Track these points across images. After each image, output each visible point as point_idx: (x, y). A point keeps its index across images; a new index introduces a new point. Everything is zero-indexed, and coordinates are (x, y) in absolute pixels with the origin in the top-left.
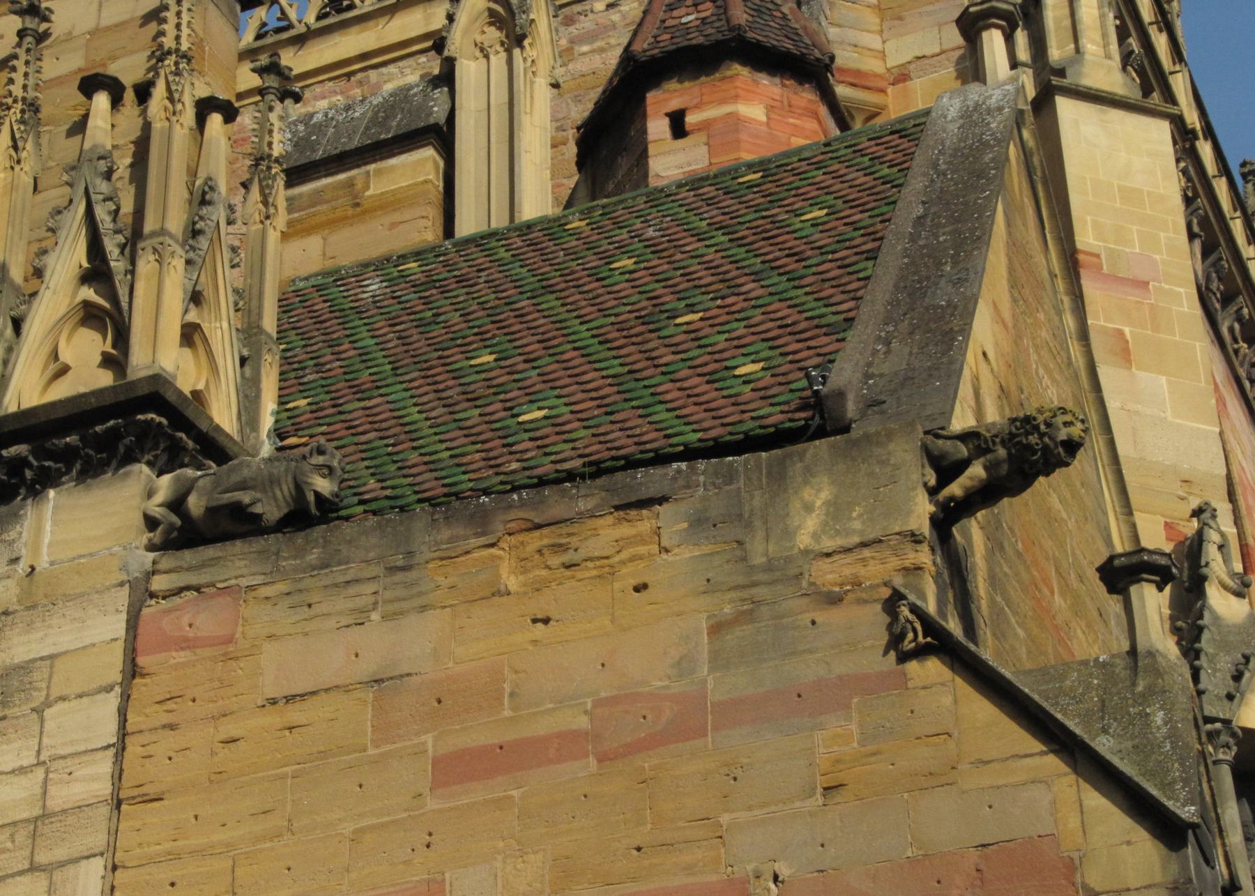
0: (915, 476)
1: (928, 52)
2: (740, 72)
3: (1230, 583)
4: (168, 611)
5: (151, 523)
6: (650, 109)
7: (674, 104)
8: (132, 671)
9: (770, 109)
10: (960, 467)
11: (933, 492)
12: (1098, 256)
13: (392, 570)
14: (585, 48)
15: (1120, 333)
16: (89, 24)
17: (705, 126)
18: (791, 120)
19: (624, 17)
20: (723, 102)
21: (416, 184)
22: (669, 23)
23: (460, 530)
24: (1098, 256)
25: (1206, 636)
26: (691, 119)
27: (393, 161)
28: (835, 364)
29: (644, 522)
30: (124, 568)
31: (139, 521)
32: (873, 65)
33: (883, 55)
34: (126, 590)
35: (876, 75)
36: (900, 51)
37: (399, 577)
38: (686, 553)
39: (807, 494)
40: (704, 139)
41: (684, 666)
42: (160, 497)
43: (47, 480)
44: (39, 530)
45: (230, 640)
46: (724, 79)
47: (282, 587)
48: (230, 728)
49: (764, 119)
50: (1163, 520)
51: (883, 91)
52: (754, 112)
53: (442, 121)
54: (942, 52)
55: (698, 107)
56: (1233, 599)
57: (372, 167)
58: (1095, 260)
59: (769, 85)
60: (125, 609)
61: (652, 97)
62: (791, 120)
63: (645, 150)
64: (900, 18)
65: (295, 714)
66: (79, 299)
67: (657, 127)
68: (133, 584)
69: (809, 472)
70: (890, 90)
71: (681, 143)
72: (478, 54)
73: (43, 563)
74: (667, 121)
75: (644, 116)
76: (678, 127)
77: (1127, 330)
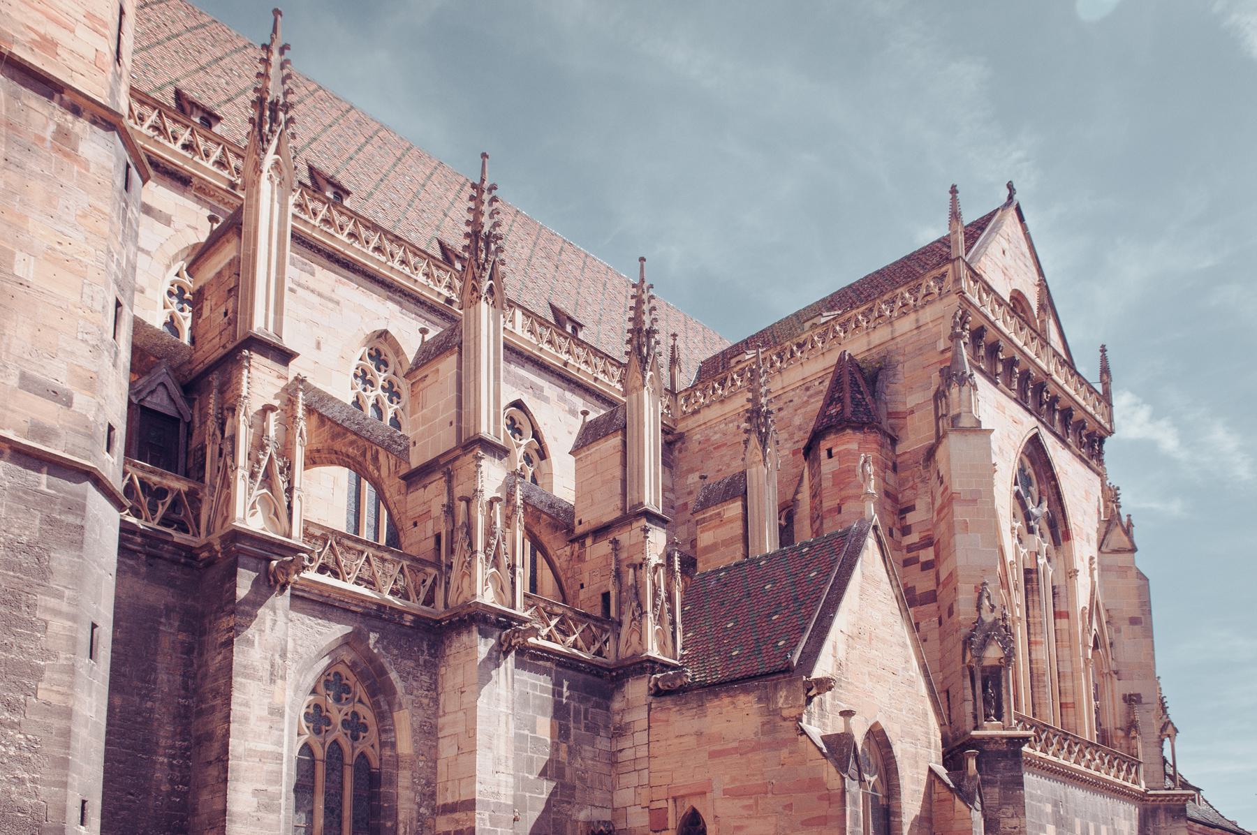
5: (650, 689)
7: (829, 446)
8: (649, 727)
9: (859, 444)
13: (699, 706)
14: (813, 400)
15: (965, 520)
17: (839, 453)
23: (712, 697)
26: (834, 451)
38: (756, 706)
41: (756, 734)
45: (668, 721)
47: (678, 708)
48: (669, 742)
65: (682, 740)
67: (824, 454)
76: (830, 455)
77: (968, 519)
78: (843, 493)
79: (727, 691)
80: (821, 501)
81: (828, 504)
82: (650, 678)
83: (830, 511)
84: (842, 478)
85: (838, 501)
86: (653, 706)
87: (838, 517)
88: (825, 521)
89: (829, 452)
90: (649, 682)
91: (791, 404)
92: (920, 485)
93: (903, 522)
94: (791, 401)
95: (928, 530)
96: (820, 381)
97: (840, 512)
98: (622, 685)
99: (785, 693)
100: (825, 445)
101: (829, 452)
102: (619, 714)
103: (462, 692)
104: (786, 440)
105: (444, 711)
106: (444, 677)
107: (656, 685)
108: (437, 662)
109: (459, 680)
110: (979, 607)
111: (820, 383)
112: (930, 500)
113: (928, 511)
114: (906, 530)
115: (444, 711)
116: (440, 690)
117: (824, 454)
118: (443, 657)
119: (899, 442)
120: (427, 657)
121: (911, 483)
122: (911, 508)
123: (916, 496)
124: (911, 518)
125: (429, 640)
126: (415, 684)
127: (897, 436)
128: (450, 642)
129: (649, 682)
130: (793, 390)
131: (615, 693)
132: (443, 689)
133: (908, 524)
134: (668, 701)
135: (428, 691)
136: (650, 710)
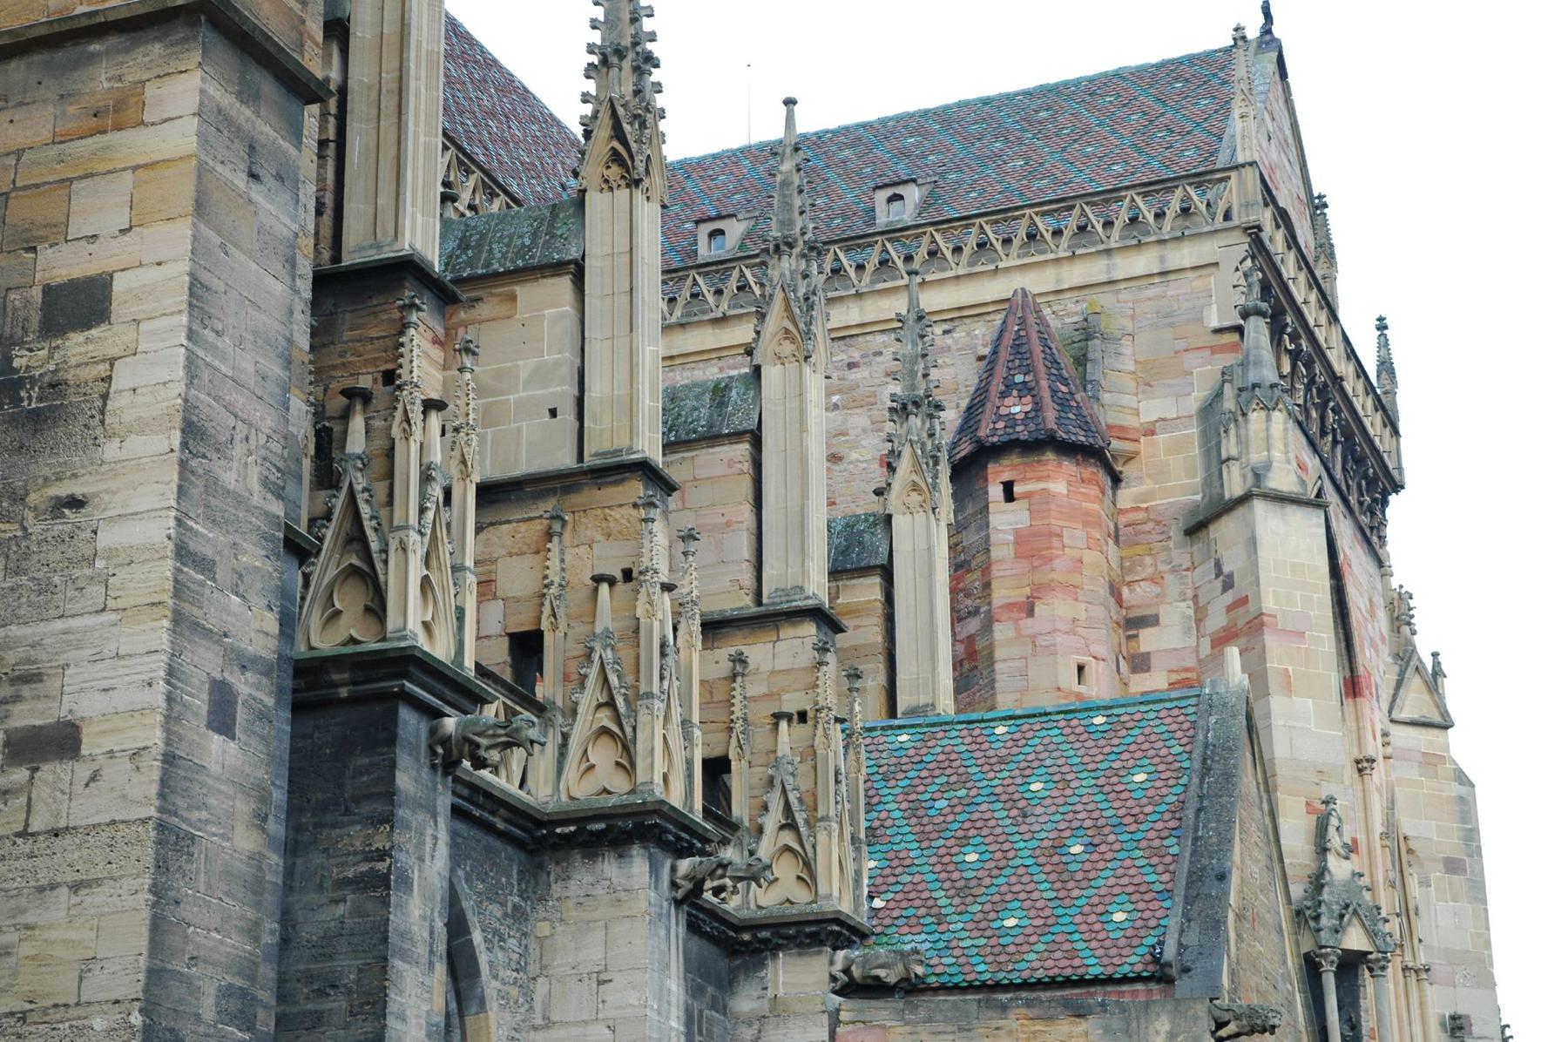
0: (1206, 1025)
1: (1169, 417)
2: (1050, 456)
3: (1342, 852)
4: (851, 1032)
5: (834, 978)
6: (990, 477)
7: (1006, 477)
10: (1226, 1024)
11: (1213, 1033)
12: (1275, 617)
13: (961, 1029)
15: (1286, 670)
16: (769, 667)
17: (1028, 495)
18: (1083, 490)
19: (956, 342)
20: (1040, 479)
21: (870, 601)
22: (1003, 411)
24: (1275, 617)
25: (1326, 890)
26: (1017, 489)
27: (854, 582)
28: (1027, 289)
29: (1082, 1026)
30: (824, 1003)
31: (826, 977)
32: (1129, 421)
33: (1137, 413)
34: (826, 1016)
35: (1134, 429)
36: (1151, 410)
37: (965, 1034)
39: (1158, 1025)
40: (1027, 506)
42: (839, 966)
43: (778, 947)
44: (776, 975)
46: (1039, 462)
47: (908, 1029)
49: (1065, 492)
50: (1304, 800)
51: (1137, 441)
52: (1059, 487)
53: (885, 562)
54: (1178, 418)
55: (1024, 480)
56: (1344, 861)
57: (841, 583)
58: (1272, 619)
59: (1069, 466)
60: (827, 1025)
61: (991, 467)
62: (1083, 490)
63: (987, 507)
64: (1150, 386)
66: (780, 844)
67: (995, 491)
68: (830, 1015)
69: (1158, 1014)
70: (1142, 439)
71: (1010, 506)
72: (906, 511)
73: (781, 993)
74: (1001, 487)
75: (986, 480)
76: (1009, 496)
77: (1290, 668)
78: (1039, 577)
79: (1029, 1004)
80: (987, 585)
81: (1002, 594)
82: (832, 957)
83: (1010, 607)
84: (1032, 547)
85: (1027, 591)
86: (844, 1016)
87: (1028, 625)
88: (997, 627)
89: (1008, 487)
90: (832, 963)
91: (879, 359)
92: (1169, 578)
93: (1133, 644)
94: (880, 353)
95: (1187, 670)
96: (946, 326)
97: (1031, 613)
98: (761, 965)
99: (1167, 1027)
100: (998, 472)
101: (1008, 487)
102: (750, 1024)
103: (600, 983)
104: (865, 431)
105: (546, 1018)
106: (547, 942)
107: (847, 971)
108: (528, 909)
109: (592, 954)
110: (1322, 850)
111: (946, 332)
112: (1191, 612)
113: (1187, 631)
114: (1140, 663)
115: (546, 1018)
116: (533, 969)
117: (995, 491)
118: (542, 899)
119: (1123, 484)
120: (517, 899)
121: (1150, 570)
122: (1149, 621)
123: (1161, 597)
124: (1148, 640)
125: (520, 863)
126: (500, 955)
127: (1121, 472)
128: (565, 870)
129: (832, 963)
130: (883, 331)
131: (741, 977)
132: (543, 967)
133: (1143, 649)
134: (881, 1011)
135: (517, 970)
136: (835, 1021)
